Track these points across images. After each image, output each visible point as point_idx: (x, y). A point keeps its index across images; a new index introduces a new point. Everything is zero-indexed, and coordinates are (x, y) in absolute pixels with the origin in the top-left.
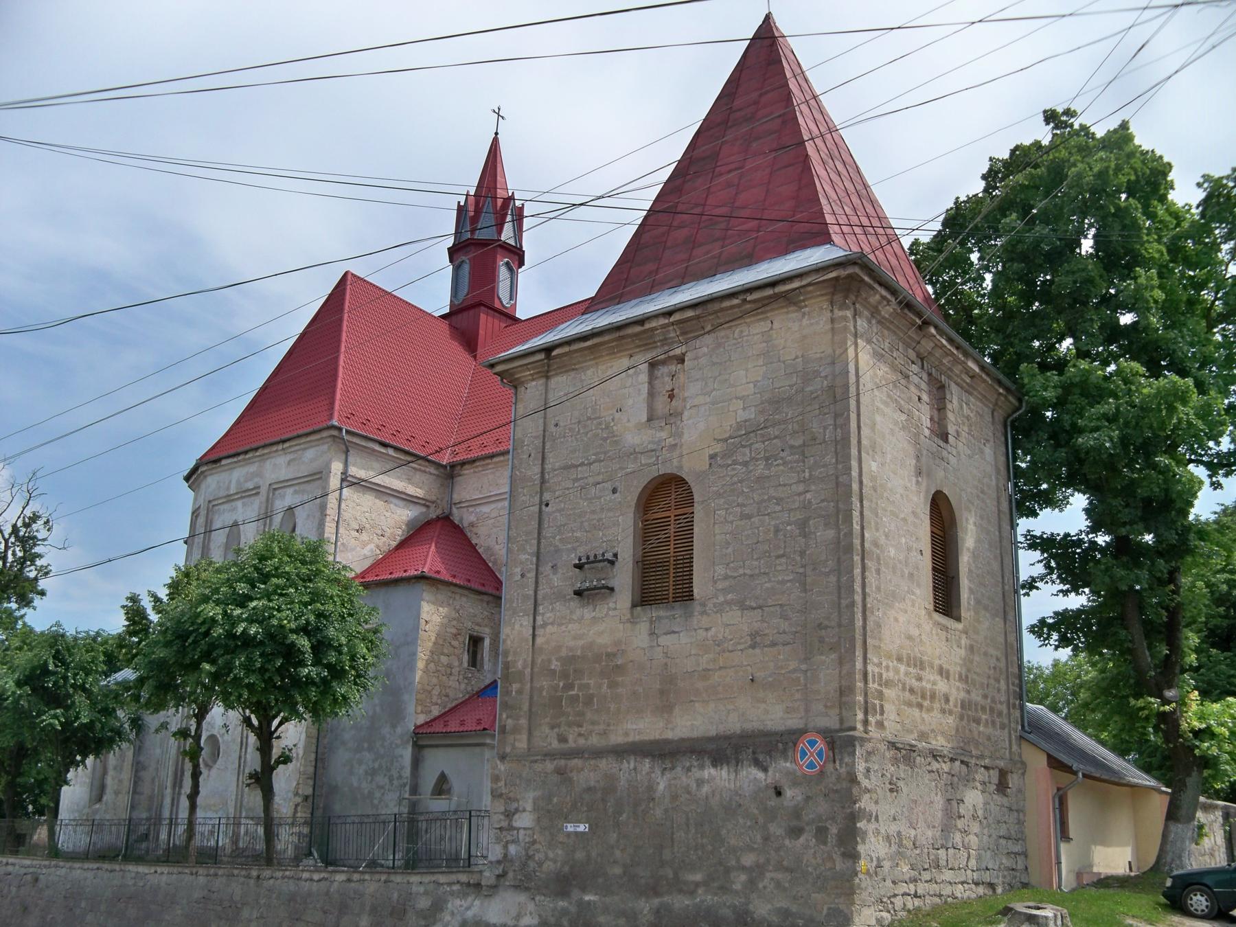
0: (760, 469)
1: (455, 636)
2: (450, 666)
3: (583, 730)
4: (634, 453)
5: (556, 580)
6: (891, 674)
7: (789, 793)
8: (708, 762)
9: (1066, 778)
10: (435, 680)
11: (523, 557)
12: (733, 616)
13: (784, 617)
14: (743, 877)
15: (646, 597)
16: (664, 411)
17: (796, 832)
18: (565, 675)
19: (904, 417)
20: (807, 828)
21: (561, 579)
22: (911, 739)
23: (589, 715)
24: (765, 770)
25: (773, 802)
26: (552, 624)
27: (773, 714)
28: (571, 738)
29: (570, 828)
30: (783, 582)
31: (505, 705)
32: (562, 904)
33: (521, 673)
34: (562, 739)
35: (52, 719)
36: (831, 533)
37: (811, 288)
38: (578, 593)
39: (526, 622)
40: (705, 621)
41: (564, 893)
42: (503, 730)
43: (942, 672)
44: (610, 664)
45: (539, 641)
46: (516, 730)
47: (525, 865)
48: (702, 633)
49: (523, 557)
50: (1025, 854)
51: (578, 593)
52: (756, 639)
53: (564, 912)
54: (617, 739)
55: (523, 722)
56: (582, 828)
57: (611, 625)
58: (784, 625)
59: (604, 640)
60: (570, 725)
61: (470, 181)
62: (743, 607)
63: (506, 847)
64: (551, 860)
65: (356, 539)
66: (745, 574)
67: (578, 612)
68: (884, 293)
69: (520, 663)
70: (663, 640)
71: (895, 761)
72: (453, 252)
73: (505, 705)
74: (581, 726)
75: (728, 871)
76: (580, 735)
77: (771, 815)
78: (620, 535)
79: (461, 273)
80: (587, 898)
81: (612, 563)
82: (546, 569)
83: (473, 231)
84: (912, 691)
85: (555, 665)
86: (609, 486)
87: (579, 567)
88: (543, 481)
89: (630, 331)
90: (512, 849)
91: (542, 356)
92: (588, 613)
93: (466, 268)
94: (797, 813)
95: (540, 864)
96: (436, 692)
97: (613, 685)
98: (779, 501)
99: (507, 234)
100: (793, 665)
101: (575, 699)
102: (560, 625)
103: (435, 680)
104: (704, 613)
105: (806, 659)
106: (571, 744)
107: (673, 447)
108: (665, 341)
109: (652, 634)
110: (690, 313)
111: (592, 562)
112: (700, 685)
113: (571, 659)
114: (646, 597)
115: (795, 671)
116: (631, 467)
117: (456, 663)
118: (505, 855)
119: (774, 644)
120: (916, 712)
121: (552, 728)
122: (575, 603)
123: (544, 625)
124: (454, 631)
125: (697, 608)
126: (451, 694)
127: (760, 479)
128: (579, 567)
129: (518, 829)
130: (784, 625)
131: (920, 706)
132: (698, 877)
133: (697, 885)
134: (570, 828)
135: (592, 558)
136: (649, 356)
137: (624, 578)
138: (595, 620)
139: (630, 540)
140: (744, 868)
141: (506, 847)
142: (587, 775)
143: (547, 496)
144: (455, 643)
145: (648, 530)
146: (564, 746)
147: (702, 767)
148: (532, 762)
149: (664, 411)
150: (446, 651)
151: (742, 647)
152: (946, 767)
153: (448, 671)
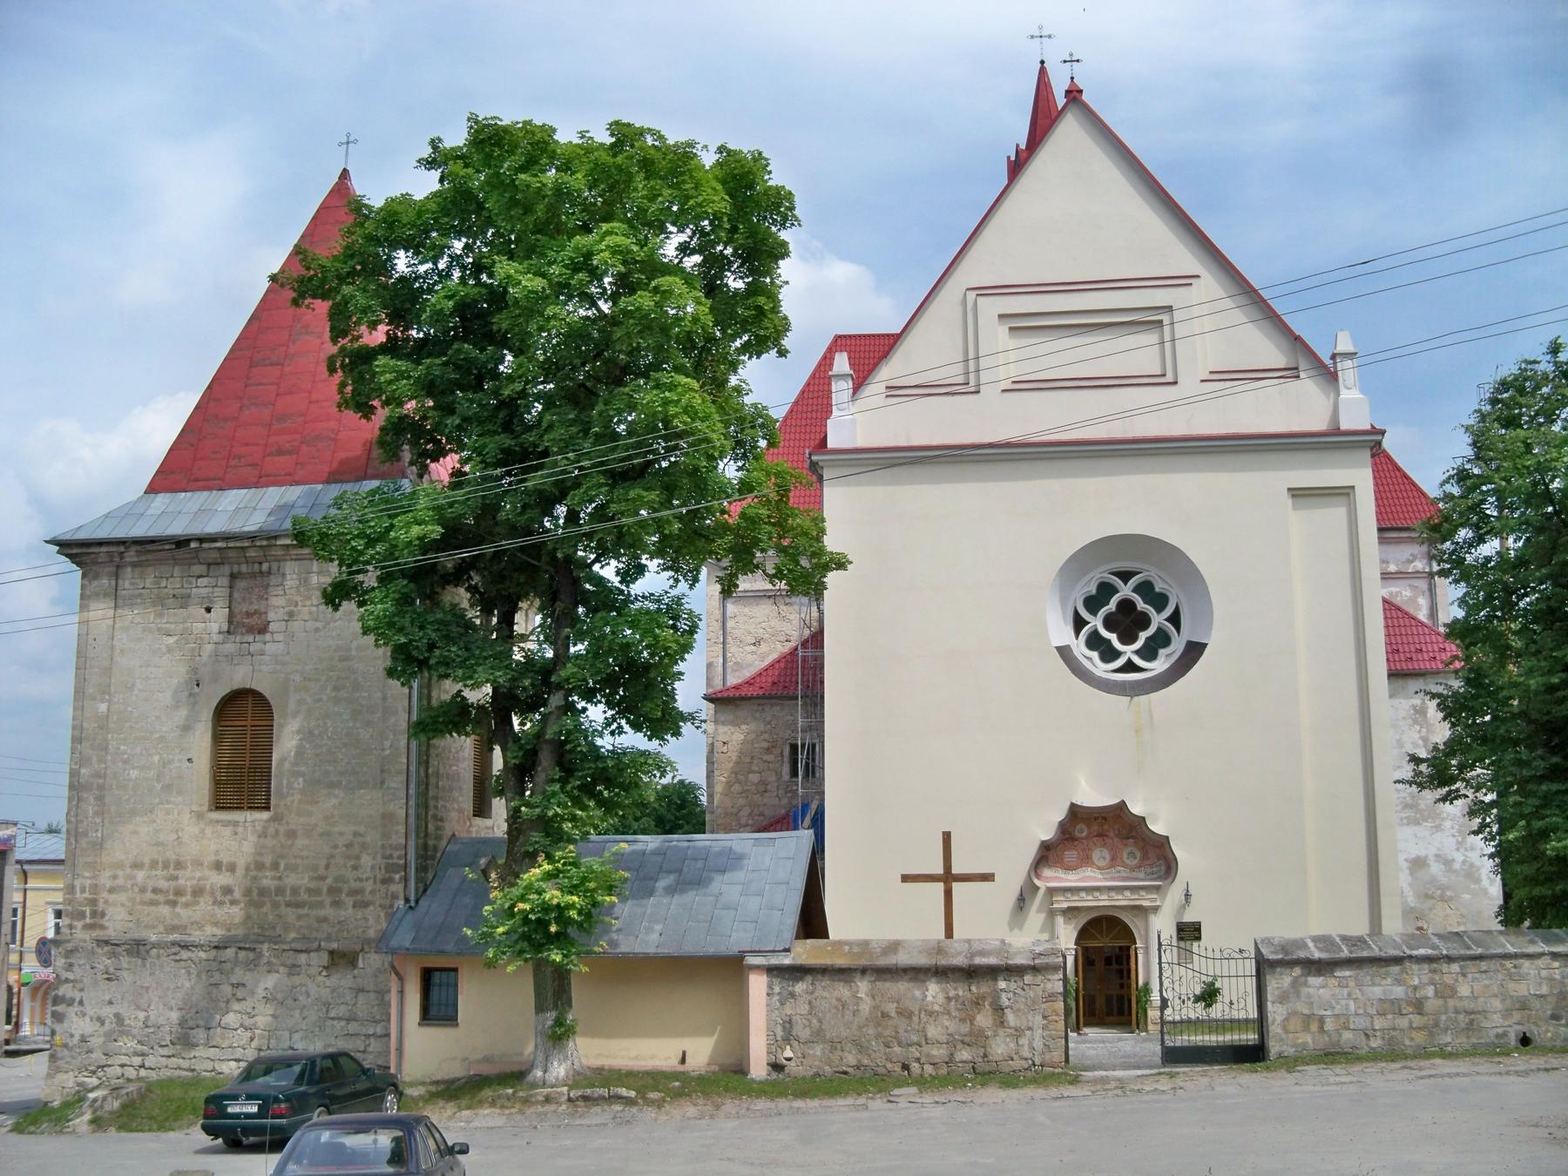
1: (768, 750)
2: (763, 783)
6: (120, 881)
10: (741, 801)
19: (171, 640)
65: (753, 653)
68: (104, 549)
71: (113, 955)
84: (155, 891)
96: (746, 811)
103: (741, 801)
117: (773, 778)
120: (165, 910)
124: (766, 745)
126: (767, 813)
131: (174, 904)
144: (770, 757)
150: (755, 768)
152: (203, 955)
153: (761, 788)
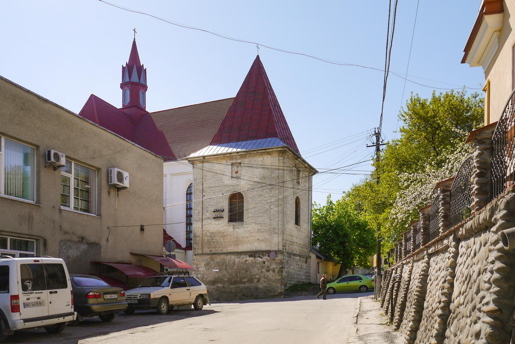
0: (260, 192)
4: (228, 186)
5: (207, 214)
7: (266, 263)
8: (248, 256)
9: (319, 260)
11: (198, 208)
12: (254, 225)
13: (266, 226)
14: (256, 280)
15: (231, 220)
16: (236, 176)
17: (268, 271)
18: (211, 236)
21: (209, 214)
22: (290, 252)
23: (218, 246)
24: (262, 258)
25: (263, 265)
27: (263, 247)
29: (214, 270)
31: (195, 243)
32: (212, 287)
33: (198, 236)
36: (277, 209)
38: (214, 218)
39: (200, 224)
40: (247, 226)
41: (213, 285)
42: (195, 249)
43: (297, 238)
44: (223, 235)
45: (204, 229)
46: (198, 249)
48: (246, 229)
49: (198, 208)
50: (310, 276)
51: (214, 218)
52: (259, 231)
53: (213, 289)
54: (225, 251)
55: (200, 247)
56: (218, 270)
57: (222, 225)
58: (266, 228)
59: (221, 229)
60: (212, 248)
61: (125, 59)
62: (256, 223)
64: (210, 278)
67: (214, 223)
69: (199, 234)
70: (236, 230)
72: (122, 86)
73: (195, 243)
75: (253, 279)
77: (263, 267)
78: (225, 205)
79: (126, 93)
81: (223, 211)
82: (205, 211)
83: (130, 78)
85: (208, 234)
86: (221, 193)
87: (214, 212)
88: (203, 190)
89: (227, 155)
92: (217, 222)
93: (128, 92)
94: (268, 267)
97: (224, 239)
98: (265, 201)
99: (142, 82)
100: (267, 236)
101: (214, 242)
104: (246, 224)
105: (271, 236)
107: (238, 185)
108: (236, 159)
109: (234, 228)
110: (244, 153)
112: (246, 240)
113: (213, 233)
114: (231, 220)
116: (227, 189)
119: (263, 232)
122: (213, 220)
123: (205, 225)
125: (245, 223)
127: (260, 195)
128: (214, 212)
130: (266, 228)
132: (246, 280)
133: (246, 282)
134: (214, 270)
136: (232, 162)
137: (226, 214)
138: (218, 224)
139: (227, 206)
140: (256, 278)
142: (218, 259)
143: (204, 194)
145: (231, 204)
149: (236, 176)
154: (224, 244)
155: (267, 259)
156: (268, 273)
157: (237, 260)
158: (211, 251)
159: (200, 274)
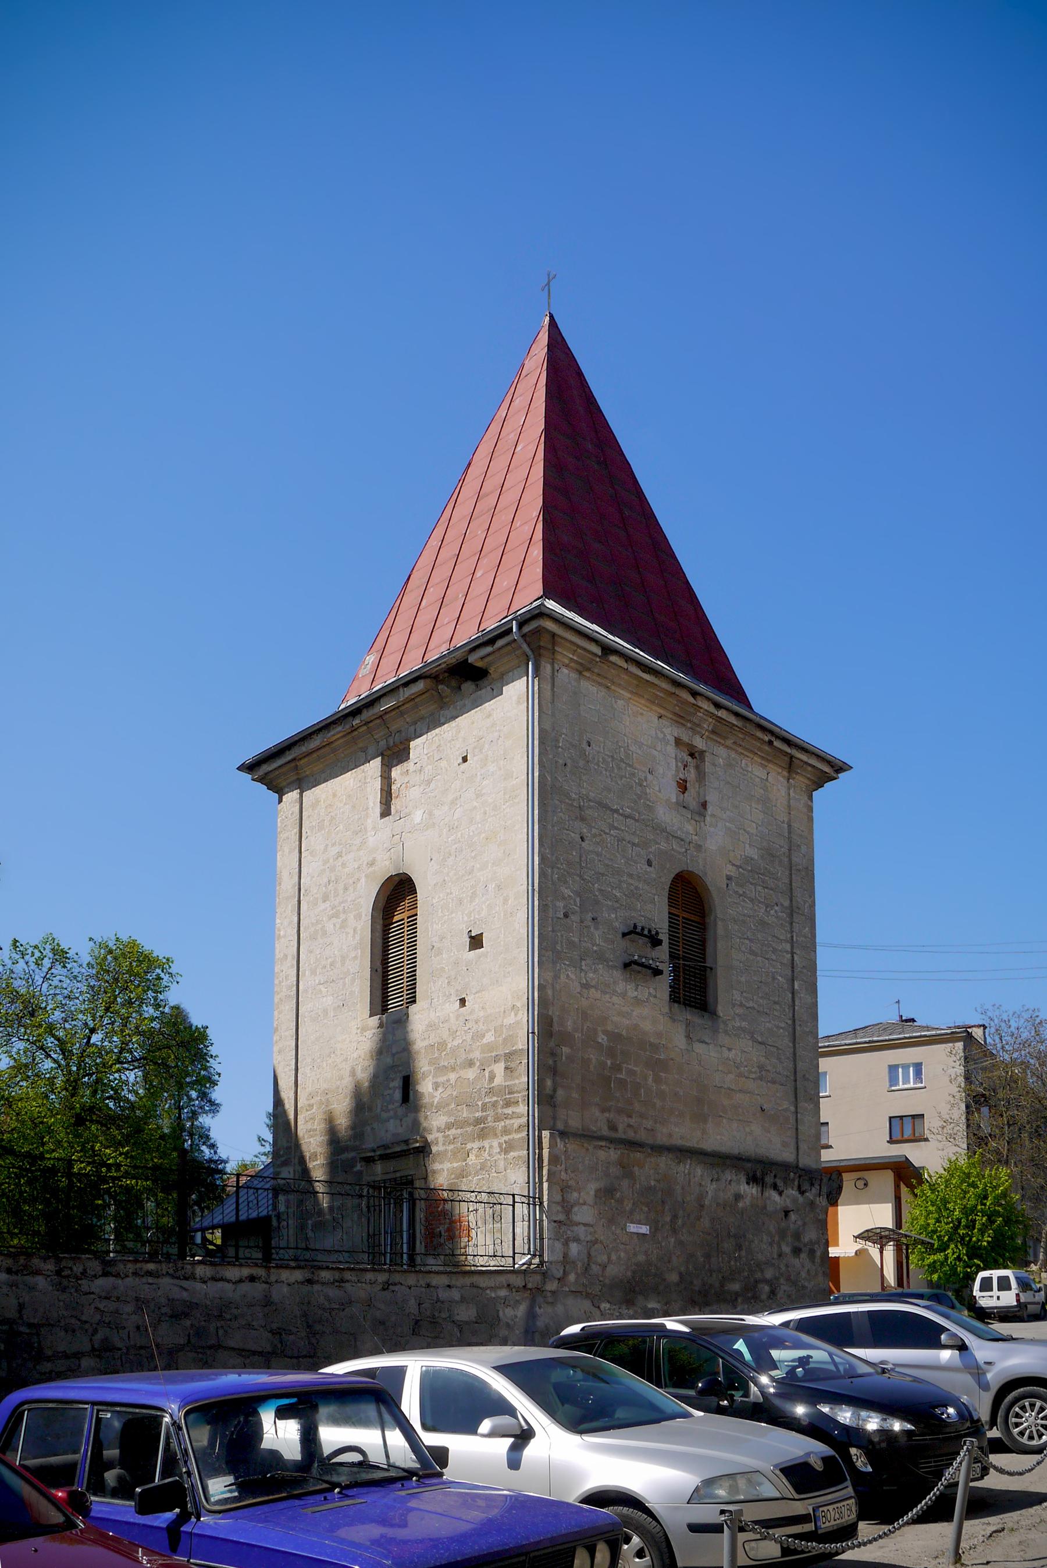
3: (632, 1121)
8: (743, 1179)
17: (796, 1251)
18: (611, 1053)
20: (804, 1249)
23: (637, 1106)
24: (780, 1194)
26: (596, 987)
28: (621, 1127)
29: (632, 1228)
30: (778, 1027)
34: (613, 1128)
35: (1037, 1038)
37: (810, 769)
47: (587, 1269)
54: (662, 1139)
56: (644, 1229)
63: (566, 1244)
66: (753, 1008)
70: (699, 1048)
74: (631, 1117)
76: (629, 1126)
80: (650, 1306)
85: (602, 1038)
90: (574, 1248)
91: (598, 651)
95: (604, 1267)
97: (657, 1080)
101: (622, 1083)
102: (604, 993)
106: (620, 1135)
111: (638, 934)
113: (619, 1036)
115: (786, 1110)
118: (565, 1256)
119: (774, 1082)
121: (603, 1111)
122: (617, 974)
129: (578, 1224)
133: (737, 1295)
134: (632, 1228)
135: (639, 930)
138: (638, 1002)
141: (566, 1244)
146: (613, 1135)
147: (738, 1182)
148: (595, 1147)
151: (753, 1076)
154: (659, 1103)
155: (795, 1200)
156: (796, 1262)
157: (711, 1188)
158: (613, 1128)
159: (577, 1240)
